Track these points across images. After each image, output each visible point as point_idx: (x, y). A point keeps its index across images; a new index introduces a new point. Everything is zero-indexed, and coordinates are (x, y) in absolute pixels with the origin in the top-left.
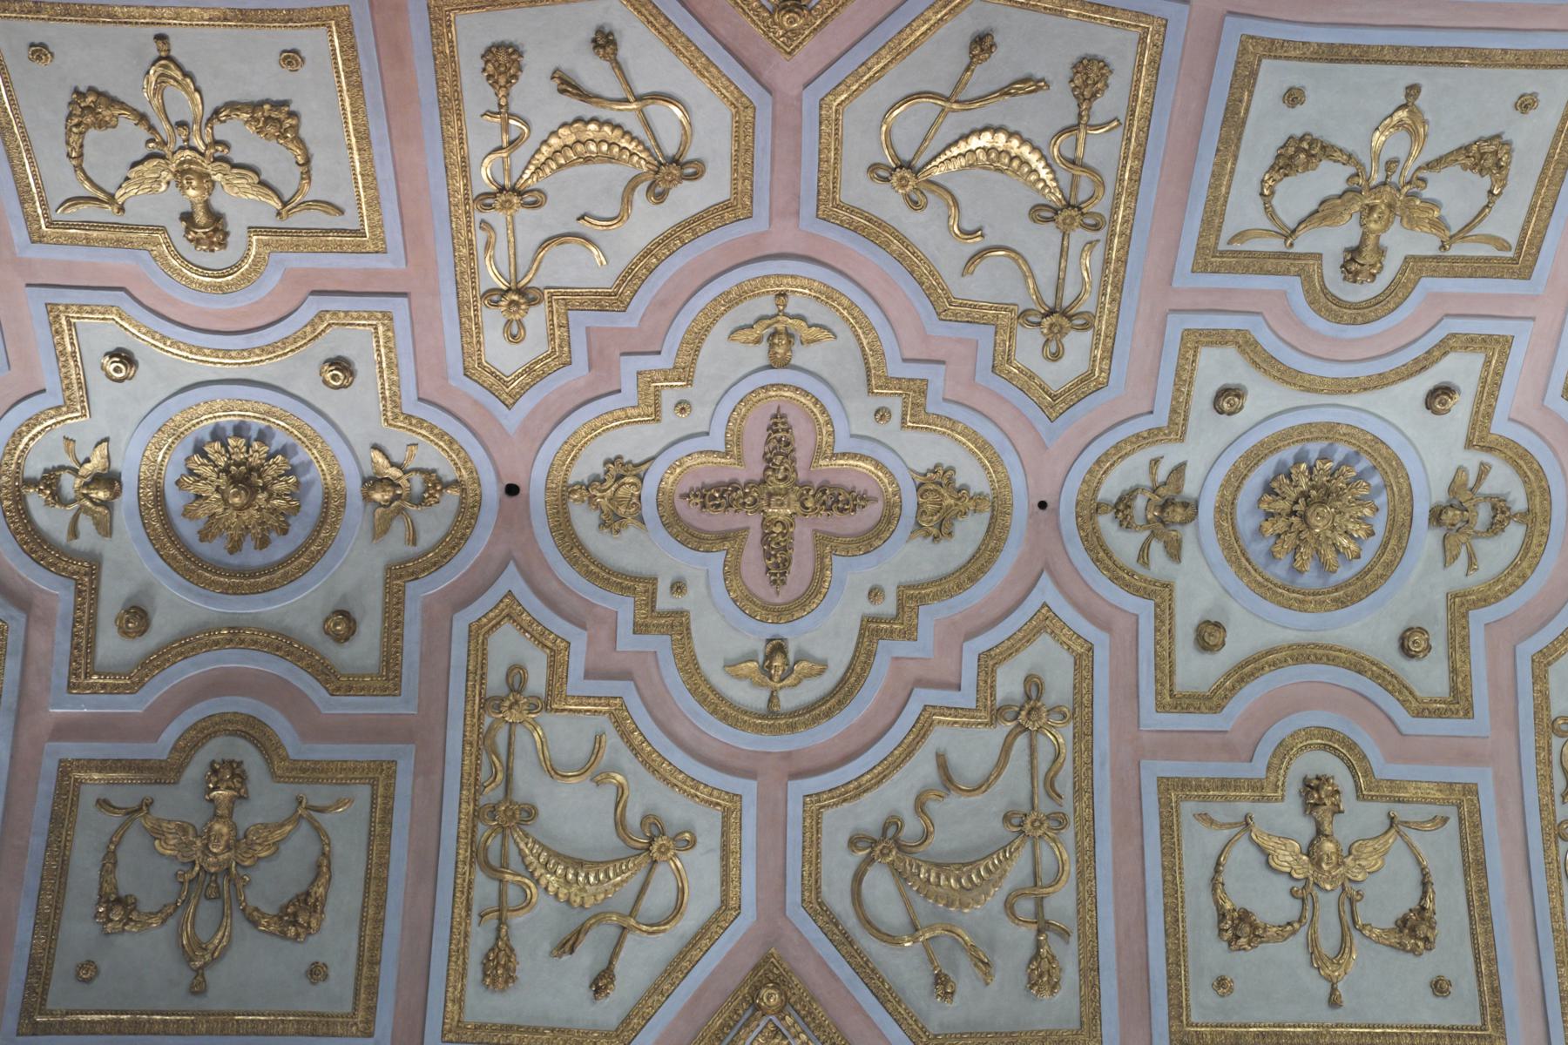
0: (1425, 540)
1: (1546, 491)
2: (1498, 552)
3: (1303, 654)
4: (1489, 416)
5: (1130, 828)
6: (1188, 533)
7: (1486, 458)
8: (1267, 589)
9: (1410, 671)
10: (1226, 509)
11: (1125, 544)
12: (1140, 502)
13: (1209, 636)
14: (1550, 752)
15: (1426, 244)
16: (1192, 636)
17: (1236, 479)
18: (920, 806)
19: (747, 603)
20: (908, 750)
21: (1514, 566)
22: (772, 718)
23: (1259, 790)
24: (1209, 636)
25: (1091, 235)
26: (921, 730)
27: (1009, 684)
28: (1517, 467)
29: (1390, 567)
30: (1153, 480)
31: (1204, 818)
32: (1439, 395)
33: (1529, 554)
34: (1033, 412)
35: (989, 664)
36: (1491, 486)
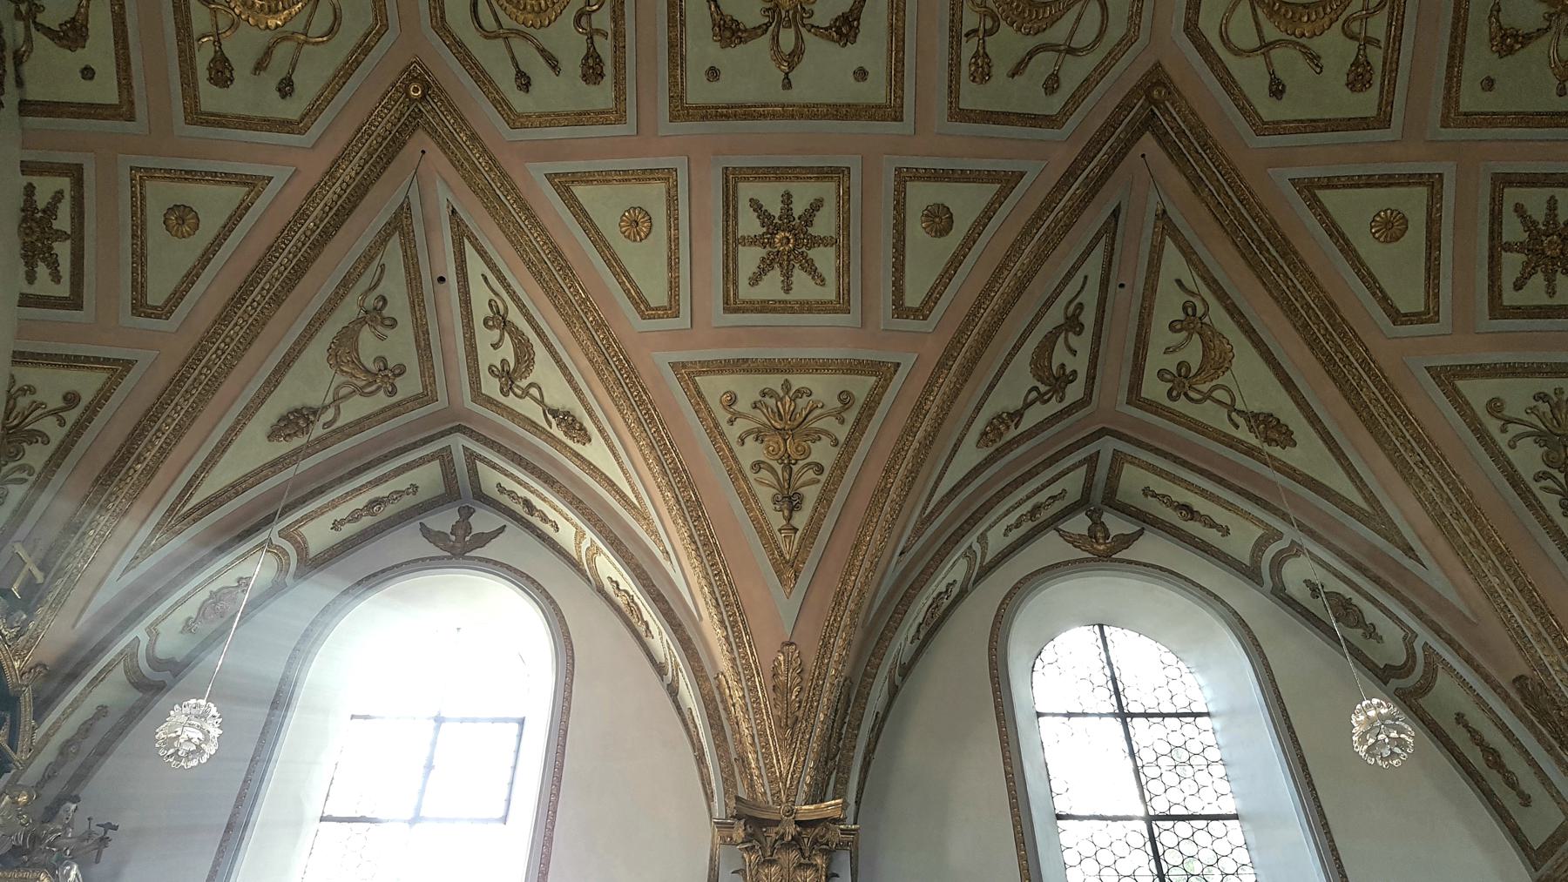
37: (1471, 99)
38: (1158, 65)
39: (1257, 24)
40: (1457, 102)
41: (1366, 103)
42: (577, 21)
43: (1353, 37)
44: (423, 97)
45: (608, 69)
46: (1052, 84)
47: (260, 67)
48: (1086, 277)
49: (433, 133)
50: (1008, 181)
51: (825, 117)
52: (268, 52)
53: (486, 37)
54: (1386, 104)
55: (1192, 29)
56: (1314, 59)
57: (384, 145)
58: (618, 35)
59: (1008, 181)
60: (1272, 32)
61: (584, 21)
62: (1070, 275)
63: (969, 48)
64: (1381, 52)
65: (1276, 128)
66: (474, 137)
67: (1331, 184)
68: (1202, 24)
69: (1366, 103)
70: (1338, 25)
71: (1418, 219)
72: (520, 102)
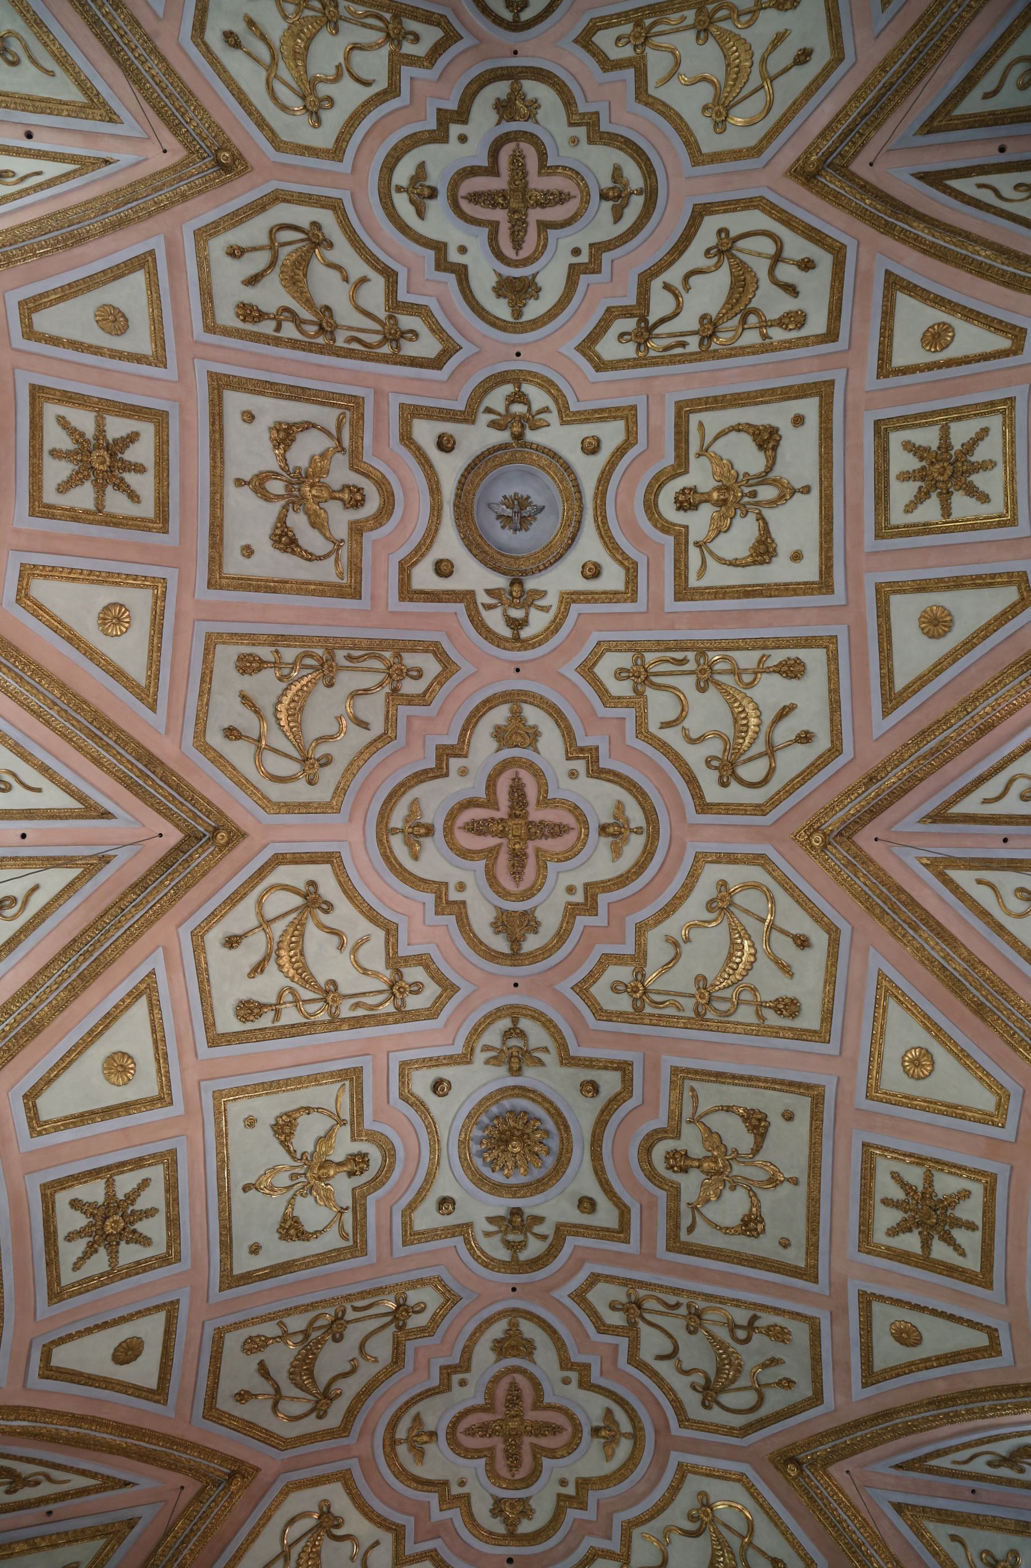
0: (530, 1077)
1: (498, 1010)
2: (536, 1035)
3: (596, 1156)
4: (451, 1057)
6: (528, 1212)
7: (478, 1049)
10: (514, 1191)
11: (534, 1248)
12: (511, 1237)
13: (587, 1204)
14: (654, 1015)
15: (344, 1133)
16: (585, 1215)
17: (497, 1189)
19: (571, 1447)
20: (654, 1375)
21: (544, 1025)
22: (637, 1436)
23: (675, 1193)
24: (587, 1204)
27: (616, 1319)
28: (483, 1030)
29: (545, 1099)
30: (496, 1233)
31: (691, 1229)
32: (439, 1087)
33: (537, 1016)
34: (456, 1309)
35: (603, 1328)
38: (244, 835)
41: (227, 1022)
42: (286, 309)
43: (280, 996)
44: (218, 163)
45: (249, 327)
47: (251, 23)
48: (39, 790)
49: (183, 164)
50: (147, 695)
51: (213, 515)
52: (263, 37)
53: (271, 231)
57: (177, 114)
58: (277, 342)
60: (278, 928)
62: (44, 770)
63: (265, 653)
64: (270, 1025)
66: (184, 197)
67: (154, 1006)
68: (282, 869)
69: (227, 1022)
70: (288, 982)
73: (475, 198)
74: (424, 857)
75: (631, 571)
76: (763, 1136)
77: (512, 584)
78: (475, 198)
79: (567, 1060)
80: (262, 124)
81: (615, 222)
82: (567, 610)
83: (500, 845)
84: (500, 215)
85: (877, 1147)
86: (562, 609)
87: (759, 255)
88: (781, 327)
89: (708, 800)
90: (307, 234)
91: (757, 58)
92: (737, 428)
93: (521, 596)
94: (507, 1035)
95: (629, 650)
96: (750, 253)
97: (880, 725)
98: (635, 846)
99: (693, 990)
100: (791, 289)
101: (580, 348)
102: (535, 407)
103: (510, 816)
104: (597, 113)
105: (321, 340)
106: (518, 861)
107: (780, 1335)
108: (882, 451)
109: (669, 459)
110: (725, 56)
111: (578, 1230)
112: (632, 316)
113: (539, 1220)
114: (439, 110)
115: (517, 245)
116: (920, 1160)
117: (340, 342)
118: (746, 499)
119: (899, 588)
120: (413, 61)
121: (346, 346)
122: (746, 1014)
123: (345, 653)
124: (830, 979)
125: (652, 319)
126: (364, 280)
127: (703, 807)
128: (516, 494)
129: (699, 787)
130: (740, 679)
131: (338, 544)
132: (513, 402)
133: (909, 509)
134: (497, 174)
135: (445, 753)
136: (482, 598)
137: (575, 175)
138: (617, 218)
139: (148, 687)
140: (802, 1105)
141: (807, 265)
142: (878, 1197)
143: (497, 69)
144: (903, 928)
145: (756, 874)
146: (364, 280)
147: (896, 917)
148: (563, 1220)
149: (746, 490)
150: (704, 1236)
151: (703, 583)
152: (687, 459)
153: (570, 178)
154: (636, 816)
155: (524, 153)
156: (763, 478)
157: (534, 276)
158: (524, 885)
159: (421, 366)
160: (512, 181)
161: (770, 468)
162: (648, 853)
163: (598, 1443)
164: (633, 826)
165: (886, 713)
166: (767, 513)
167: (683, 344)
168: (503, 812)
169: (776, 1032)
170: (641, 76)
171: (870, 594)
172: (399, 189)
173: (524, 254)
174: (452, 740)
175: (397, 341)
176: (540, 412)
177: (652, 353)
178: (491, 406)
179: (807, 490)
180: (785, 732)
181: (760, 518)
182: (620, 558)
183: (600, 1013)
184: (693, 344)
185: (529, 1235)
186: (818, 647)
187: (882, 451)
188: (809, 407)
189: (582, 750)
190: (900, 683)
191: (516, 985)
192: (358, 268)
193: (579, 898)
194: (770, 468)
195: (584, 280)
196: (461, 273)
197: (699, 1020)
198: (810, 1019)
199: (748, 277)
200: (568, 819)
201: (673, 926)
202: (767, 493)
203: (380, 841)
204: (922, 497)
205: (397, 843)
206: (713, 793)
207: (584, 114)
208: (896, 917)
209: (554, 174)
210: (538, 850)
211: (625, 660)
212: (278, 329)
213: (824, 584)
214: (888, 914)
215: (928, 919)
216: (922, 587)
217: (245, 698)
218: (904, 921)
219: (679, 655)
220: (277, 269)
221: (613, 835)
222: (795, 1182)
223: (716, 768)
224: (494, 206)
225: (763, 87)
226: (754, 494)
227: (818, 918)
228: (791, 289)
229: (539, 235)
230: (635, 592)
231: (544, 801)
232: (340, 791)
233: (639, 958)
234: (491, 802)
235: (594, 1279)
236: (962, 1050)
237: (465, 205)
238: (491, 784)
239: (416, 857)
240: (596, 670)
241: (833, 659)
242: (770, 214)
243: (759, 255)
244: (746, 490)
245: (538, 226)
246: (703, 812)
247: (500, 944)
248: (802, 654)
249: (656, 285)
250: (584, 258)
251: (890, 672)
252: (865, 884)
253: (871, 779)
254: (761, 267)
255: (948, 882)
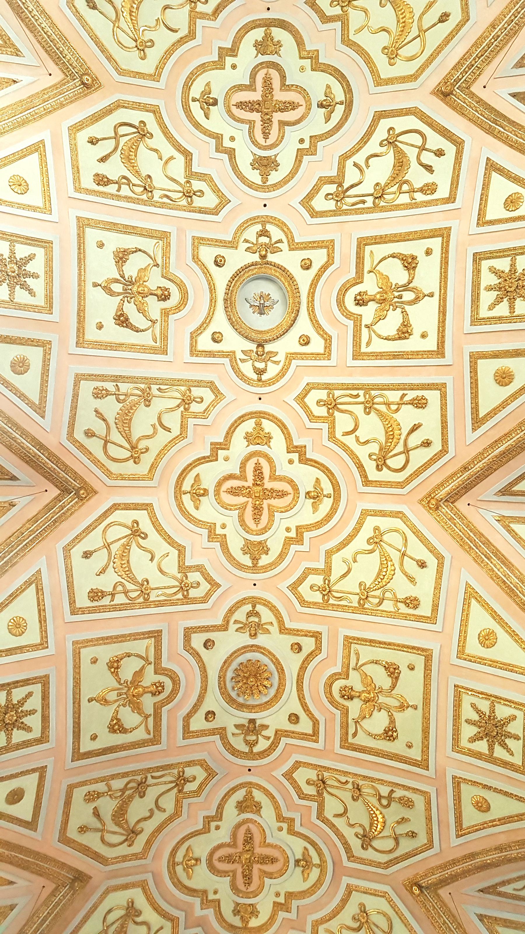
0: (261, 640)
2: (266, 615)
5: (358, 762)
8: (277, 696)
9: (306, 651)
11: (262, 745)
13: (294, 718)
14: (335, 605)
16: (292, 725)
18: (352, 826)
19: (281, 873)
20: (332, 826)
22: (322, 866)
23: (345, 712)
25: (149, 778)
26: (325, 821)
27: (311, 790)
29: (270, 652)
31: (355, 735)
33: (267, 604)
35: (302, 796)
36: (243, 619)
37: (87, 653)
38: (96, 493)
39: (119, 539)
40: (86, 647)
41: (82, 601)
42: (124, 177)
43: (115, 588)
44: (83, 83)
45: (101, 188)
46: (90, 434)
49: (62, 83)
51: (79, 304)
53: (115, 127)
54: (83, 611)
55: (115, 507)
56: (103, 571)
57: (57, 51)
58: (119, 198)
59: (40, 410)
60: (114, 548)
61: (124, 181)
63: (110, 386)
64: (108, 603)
65: (67, 557)
66: (62, 105)
69: (82, 601)
71: (22, 641)
72: (83, 136)
73: (240, 105)
74: (201, 508)
75: (328, 341)
76: (397, 678)
77: (257, 347)
78: (240, 105)
79: (283, 630)
80: (110, 58)
81: (326, 123)
82: (290, 364)
83: (247, 502)
84: (256, 117)
85: (462, 688)
86: (287, 363)
87: (412, 145)
88: (422, 192)
89: (370, 479)
90: (137, 129)
91: (416, 18)
92: (393, 256)
93: (263, 355)
94: (249, 615)
95: (325, 389)
96: (407, 144)
97: (471, 436)
98: (326, 504)
99: (358, 591)
100: (429, 168)
101: (302, 203)
102: (274, 240)
103: (253, 485)
104: (318, 51)
105: (144, 197)
106: (258, 511)
107: (408, 804)
108: (477, 272)
109: (353, 274)
110: (397, 15)
111: (287, 734)
112: (334, 183)
113: (265, 727)
114: (220, 48)
115: (266, 135)
116: (487, 696)
117: (156, 198)
118: (396, 300)
119: (484, 356)
120: (203, 16)
121: (160, 200)
122: (388, 606)
123: (158, 387)
124: (438, 587)
125: (346, 185)
126: (171, 158)
127: (367, 482)
128: (262, 292)
129: (365, 471)
130: (389, 407)
131: (154, 322)
132: (261, 235)
133: (491, 308)
134: (255, 90)
135: (216, 447)
136: (240, 355)
137: (302, 91)
138: (328, 119)
139: (40, 404)
140: (419, 661)
141: (440, 153)
142: (463, 718)
143: (256, 20)
144: (481, 557)
145: (397, 523)
146: (171, 158)
147: (478, 551)
148: (279, 728)
149: (396, 294)
150: (362, 740)
151: (369, 350)
152: (363, 274)
153: (300, 93)
154: (327, 487)
155: (272, 76)
156: (406, 287)
157: (276, 156)
158: (260, 526)
159: (206, 213)
160: (264, 96)
161: (410, 282)
162: (334, 510)
163: (299, 870)
164: (325, 493)
165: (474, 430)
166: (407, 308)
167: (364, 202)
168: (250, 482)
169: (406, 617)
170: (345, 27)
171: (467, 359)
172: (194, 100)
173: (270, 142)
174: (220, 439)
175: (191, 197)
176: (276, 242)
177: (345, 207)
178: (247, 238)
179: (431, 295)
180: (415, 440)
181: (404, 312)
182: (322, 333)
183: (303, 602)
184: (370, 200)
185: (259, 736)
186: (435, 389)
187: (477, 272)
188: (436, 243)
189: (296, 447)
190: (482, 413)
191: (255, 585)
192: (168, 150)
193: (293, 534)
194: (410, 282)
195: (306, 159)
196: (231, 153)
197: (361, 608)
198: (425, 610)
199: (405, 160)
200: (287, 487)
201: (348, 552)
202: (408, 296)
203: (176, 497)
204: (499, 300)
205: (186, 499)
206: (373, 474)
207: (309, 52)
208: (478, 551)
209: (290, 90)
210: (269, 506)
211: (323, 394)
212: (119, 190)
213: (440, 352)
214: (473, 549)
215: (497, 553)
216: (496, 355)
217: (96, 411)
218: (483, 554)
219: (355, 393)
220: (119, 152)
221: (314, 498)
222: (415, 708)
223: (375, 460)
224: (252, 110)
225: (420, 36)
226: (400, 297)
227: (433, 550)
228: (429, 168)
229: (279, 130)
230: (330, 354)
231: (273, 477)
232: (153, 467)
233: (327, 571)
234: (243, 477)
235: (297, 765)
236: (514, 631)
237: (234, 110)
238: (243, 466)
239: (197, 508)
240: (306, 400)
241: (444, 397)
242: (421, 120)
243: (412, 145)
244: (396, 294)
245: (279, 124)
246: (366, 485)
247: (246, 560)
248: (426, 393)
249: (349, 163)
250: (306, 145)
251: (477, 404)
252: (460, 531)
253: (465, 468)
254: (412, 153)
255: (510, 531)
